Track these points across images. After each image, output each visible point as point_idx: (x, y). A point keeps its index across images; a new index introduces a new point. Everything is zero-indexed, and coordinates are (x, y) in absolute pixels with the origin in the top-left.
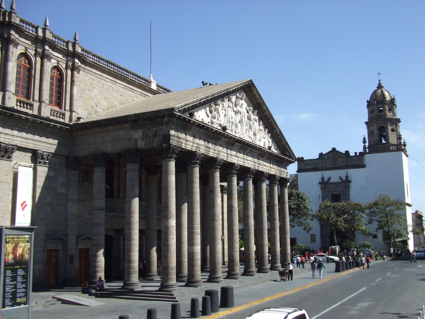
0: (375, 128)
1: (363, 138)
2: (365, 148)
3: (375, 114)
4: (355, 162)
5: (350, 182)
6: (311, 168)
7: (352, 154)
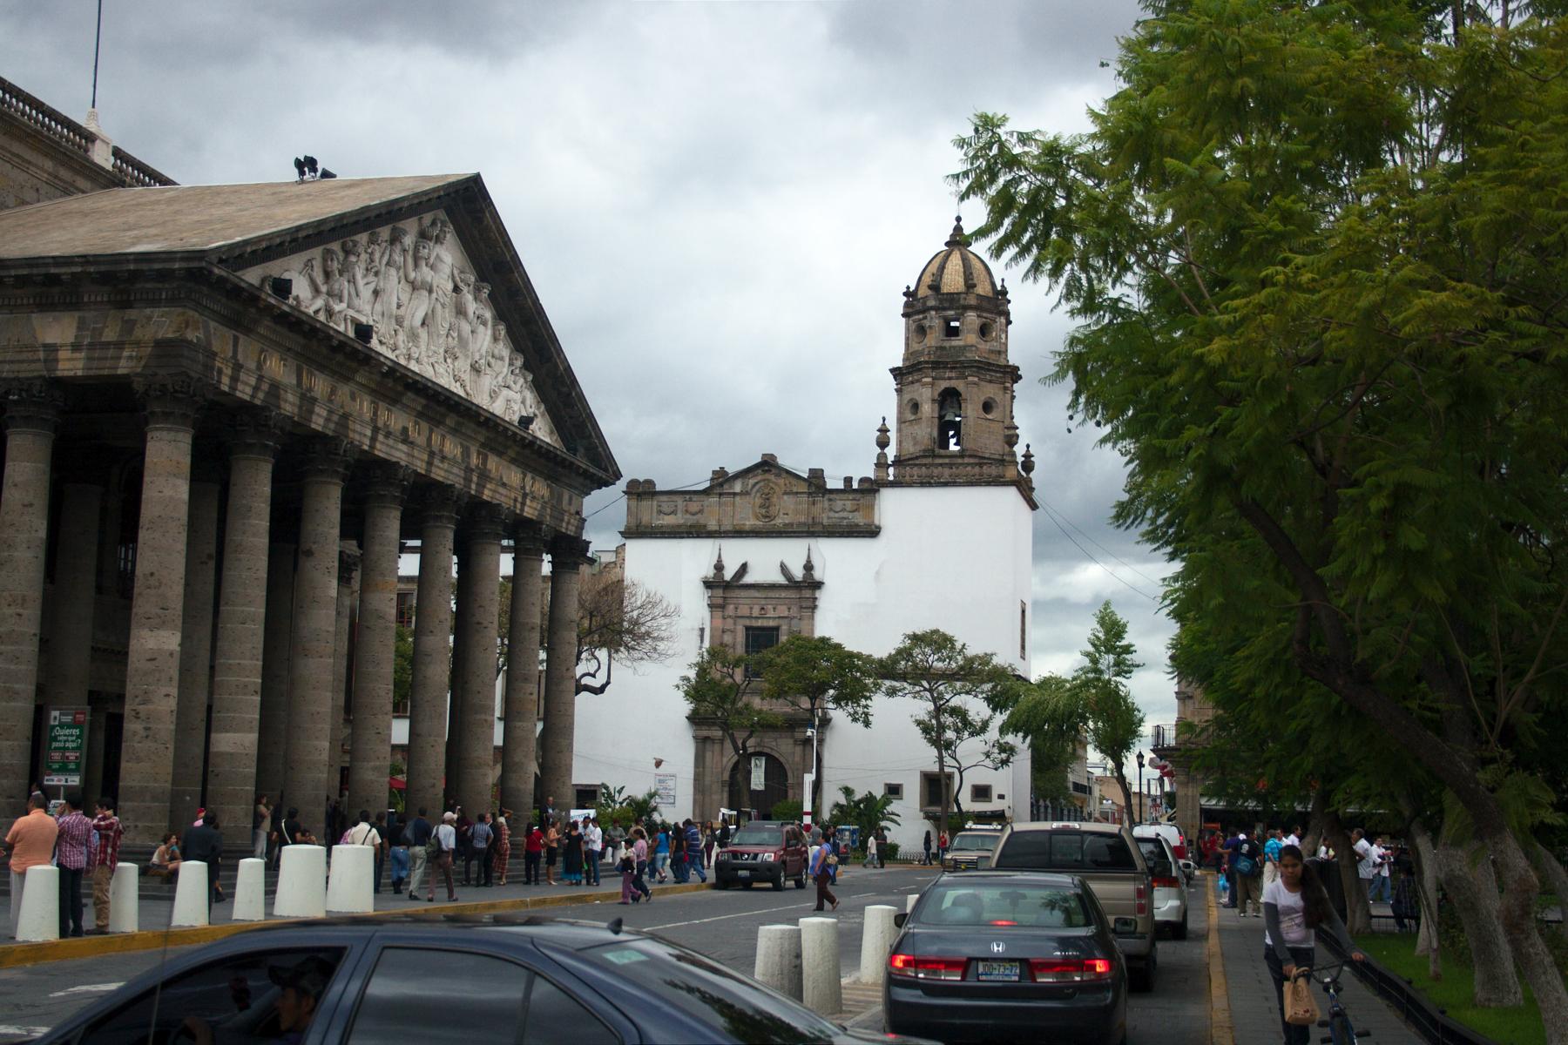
0: (926, 395)
1: (879, 425)
2: (881, 464)
3: (934, 339)
4: (842, 514)
5: (818, 585)
6: (679, 526)
7: (835, 482)
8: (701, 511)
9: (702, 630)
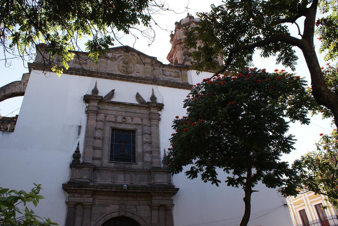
9: (80, 127)
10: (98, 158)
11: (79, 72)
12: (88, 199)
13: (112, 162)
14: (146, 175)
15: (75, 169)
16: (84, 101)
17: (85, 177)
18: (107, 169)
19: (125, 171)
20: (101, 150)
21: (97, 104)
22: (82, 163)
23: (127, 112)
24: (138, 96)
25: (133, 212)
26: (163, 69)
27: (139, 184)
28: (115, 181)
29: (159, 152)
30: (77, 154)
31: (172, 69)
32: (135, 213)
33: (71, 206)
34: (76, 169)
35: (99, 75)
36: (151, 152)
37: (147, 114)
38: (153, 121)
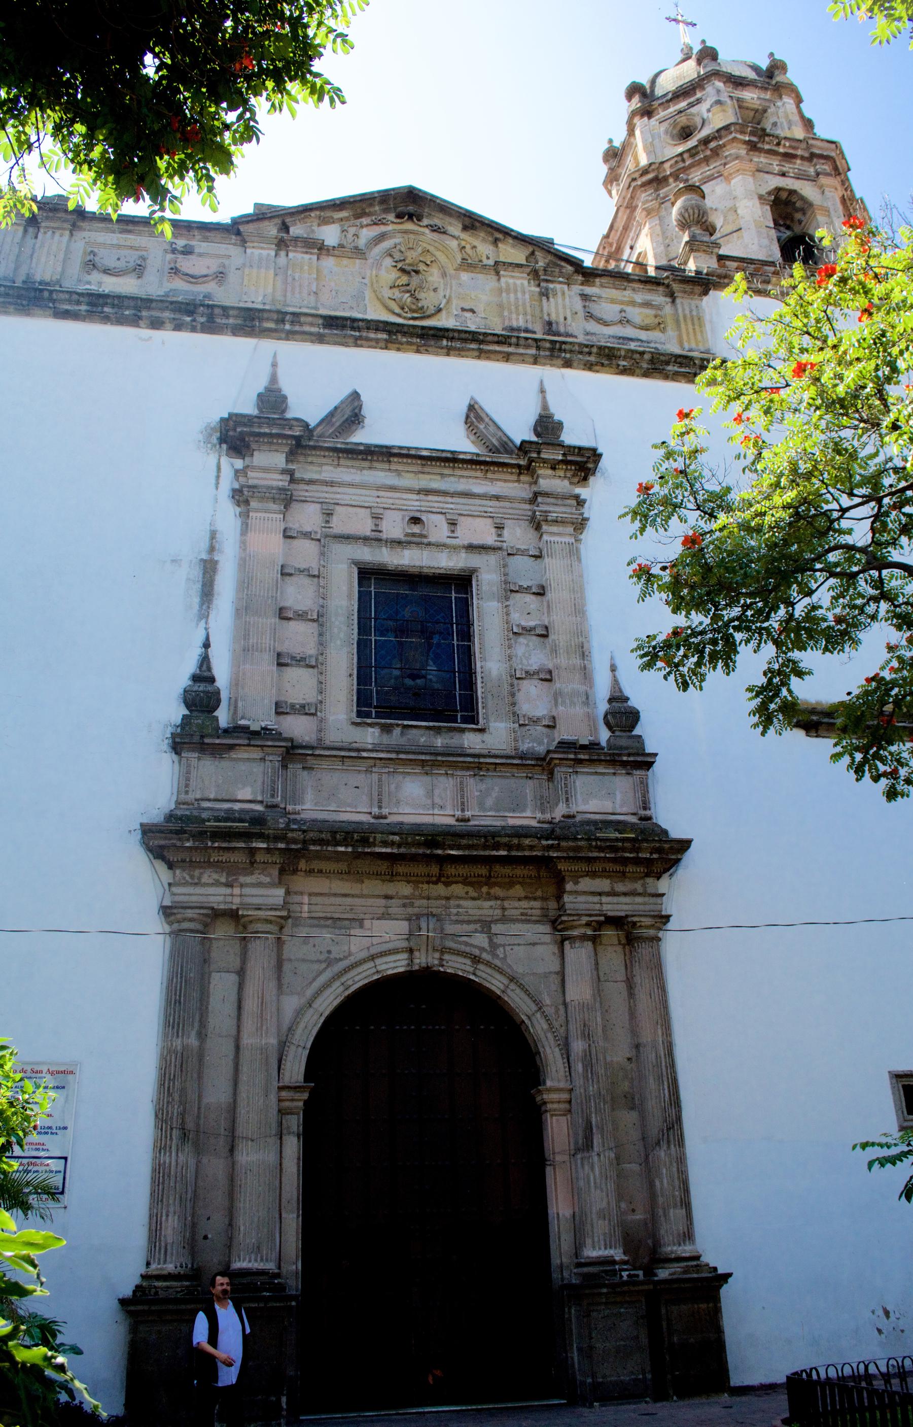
8: (220, 276)
10: (303, 706)
11: (190, 313)
12: (260, 893)
13: (369, 721)
14: (530, 781)
15: (197, 755)
16: (224, 446)
17: (245, 793)
18: (349, 755)
19: (431, 762)
20: (313, 667)
21: (284, 460)
22: (226, 731)
23: (428, 492)
24: (474, 416)
25: (477, 952)
26: (588, 290)
27: (503, 823)
28: (385, 811)
29: (586, 674)
30: (202, 687)
31: (627, 293)
32: (485, 956)
33: (186, 925)
34: (199, 759)
35: (287, 327)
36: (548, 677)
37: (524, 501)
38: (554, 529)
